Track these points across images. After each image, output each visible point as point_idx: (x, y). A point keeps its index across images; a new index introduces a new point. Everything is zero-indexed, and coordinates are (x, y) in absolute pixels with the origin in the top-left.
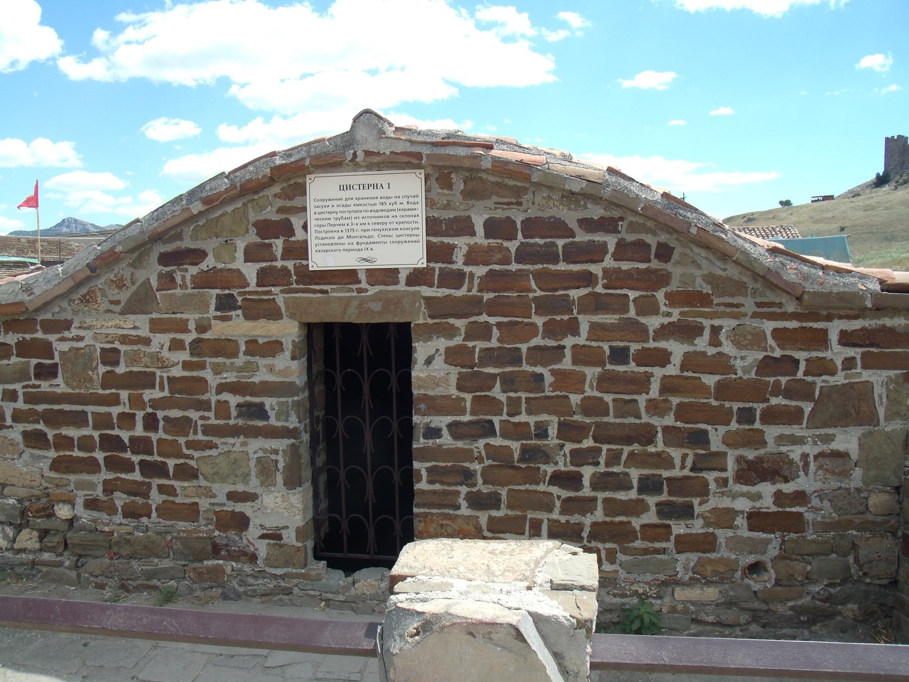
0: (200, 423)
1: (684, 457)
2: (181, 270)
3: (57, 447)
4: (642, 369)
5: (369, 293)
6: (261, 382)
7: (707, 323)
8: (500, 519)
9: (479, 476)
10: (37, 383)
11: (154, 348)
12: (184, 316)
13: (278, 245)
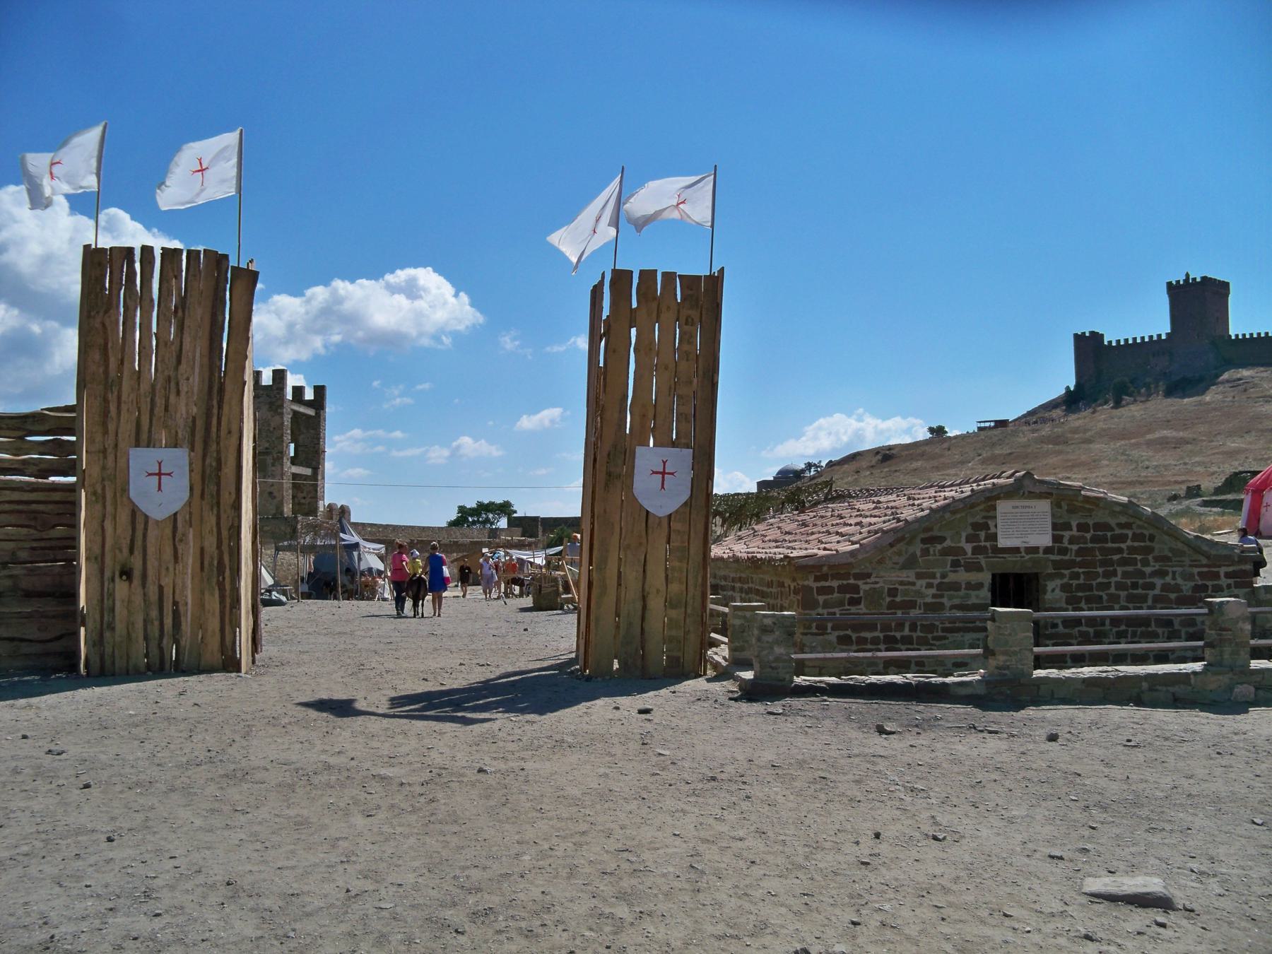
0: (940, 626)
1: (1163, 633)
4: (1144, 592)
7: (1170, 570)
11: (917, 587)
12: (935, 570)
13: (982, 534)
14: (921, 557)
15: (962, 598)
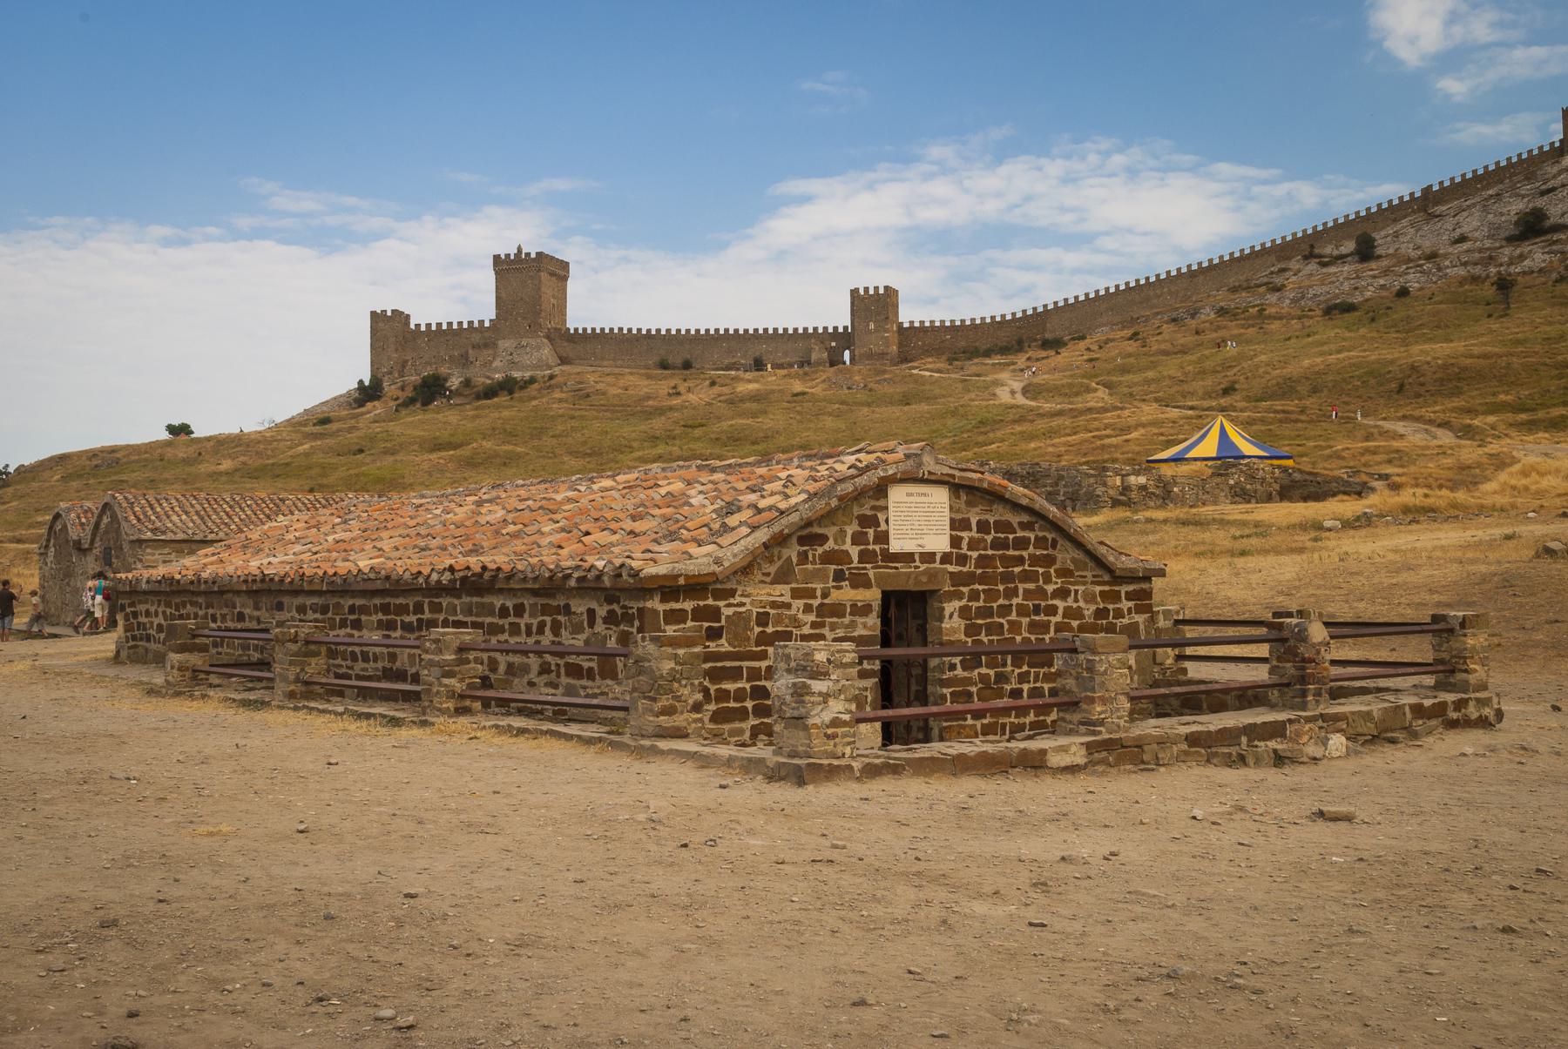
3: (718, 700)
4: (1046, 618)
6: (859, 636)
7: (1072, 588)
8: (987, 725)
12: (814, 586)
13: (871, 532)
14: (797, 565)
15: (847, 627)
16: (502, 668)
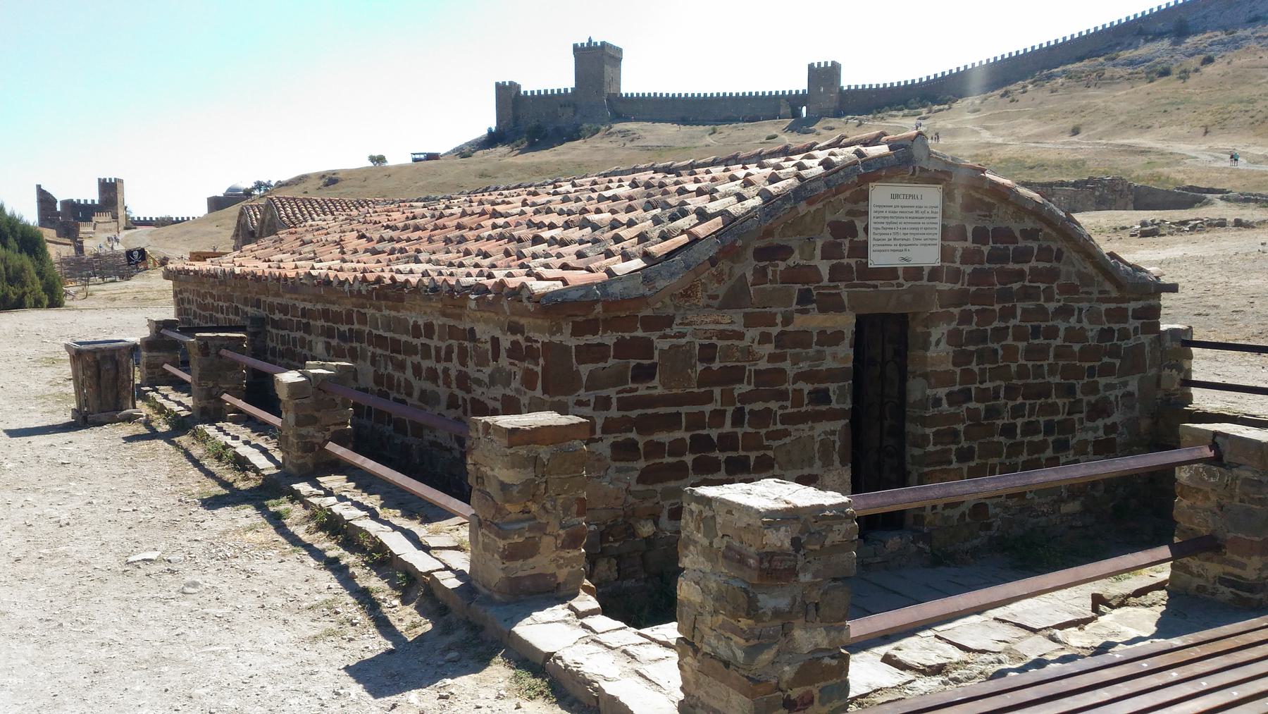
1: (1064, 406)
2: (774, 266)
5: (904, 287)
6: (826, 370)
7: (1076, 305)
9: (962, 434)
10: (635, 386)
11: (746, 343)
12: (774, 310)
13: (846, 243)
16: (416, 394)
